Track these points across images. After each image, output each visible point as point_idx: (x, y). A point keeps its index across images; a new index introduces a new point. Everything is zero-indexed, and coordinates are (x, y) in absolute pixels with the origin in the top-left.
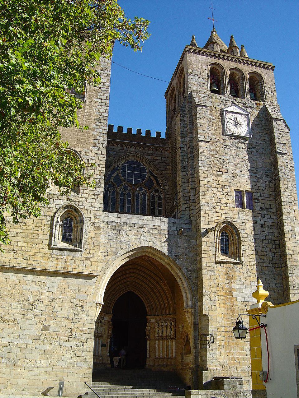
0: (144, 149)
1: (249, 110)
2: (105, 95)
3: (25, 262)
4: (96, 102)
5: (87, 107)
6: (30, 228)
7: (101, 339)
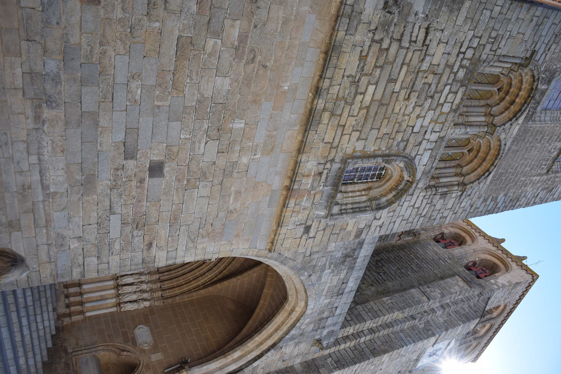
3: (330, 106)
6: (397, 110)
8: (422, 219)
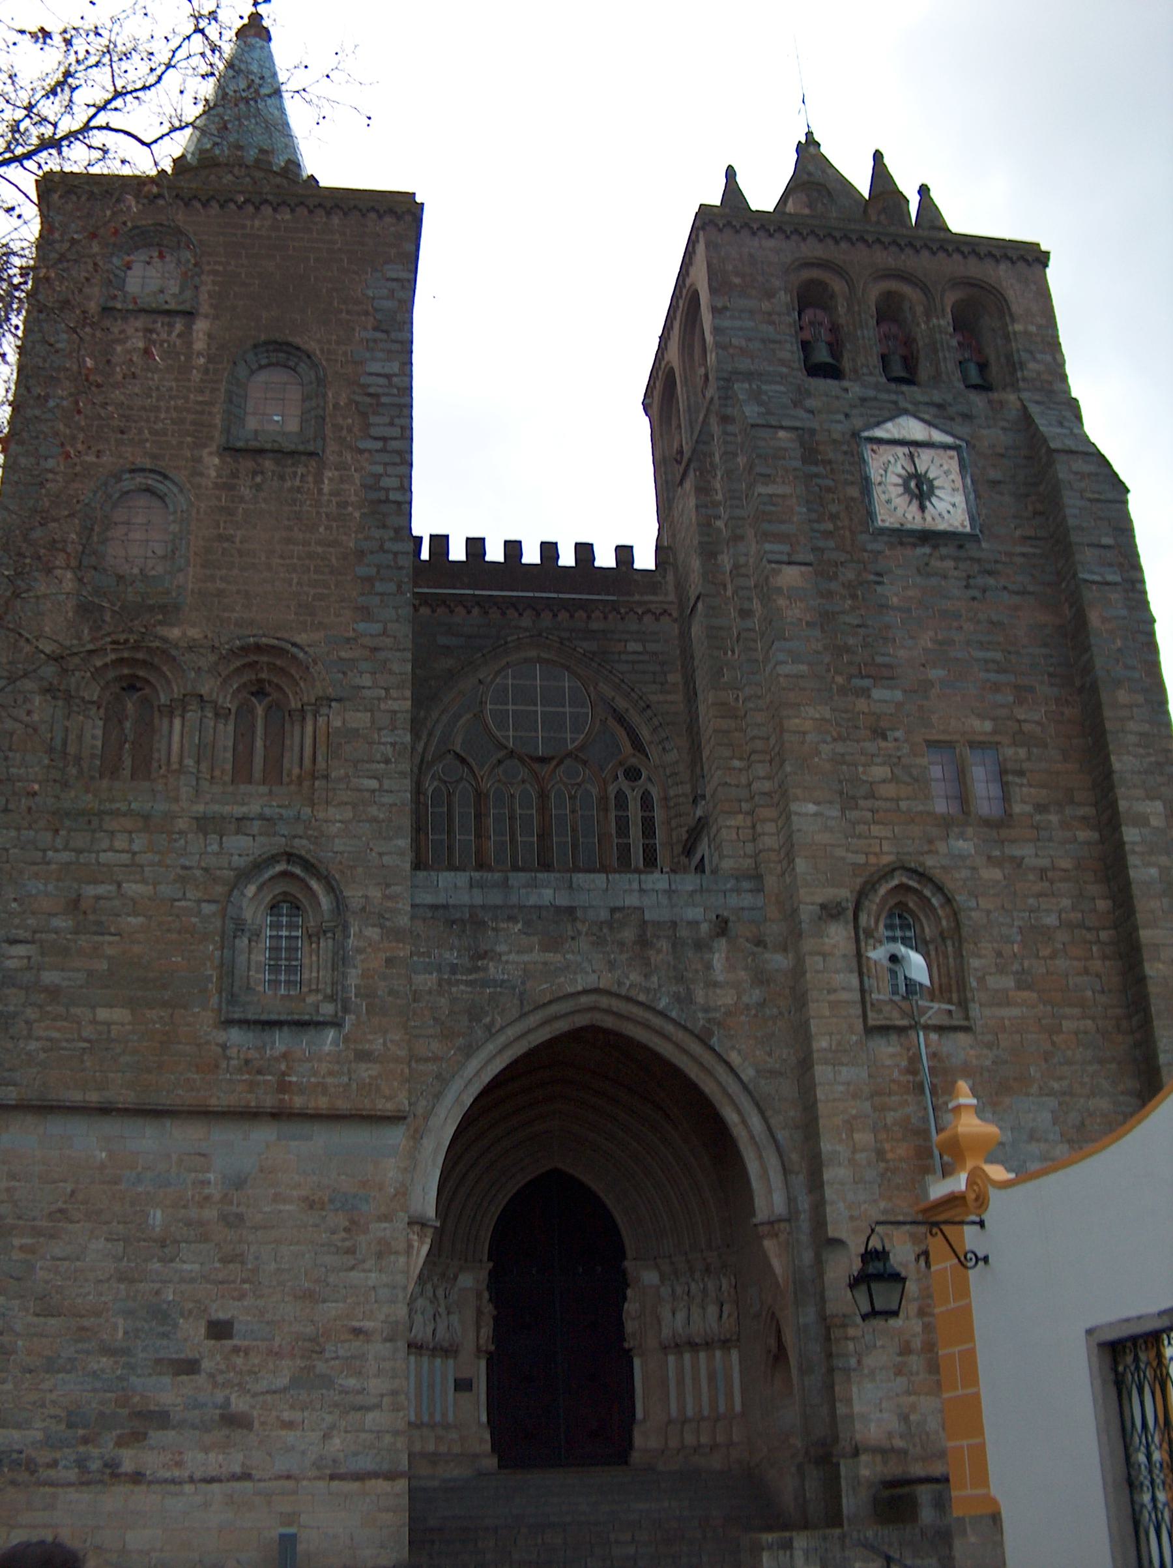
0: (572, 616)
1: (964, 430)
2: (397, 421)
4: (361, 451)
5: (328, 474)
7: (451, 1362)
8: (387, 784)
